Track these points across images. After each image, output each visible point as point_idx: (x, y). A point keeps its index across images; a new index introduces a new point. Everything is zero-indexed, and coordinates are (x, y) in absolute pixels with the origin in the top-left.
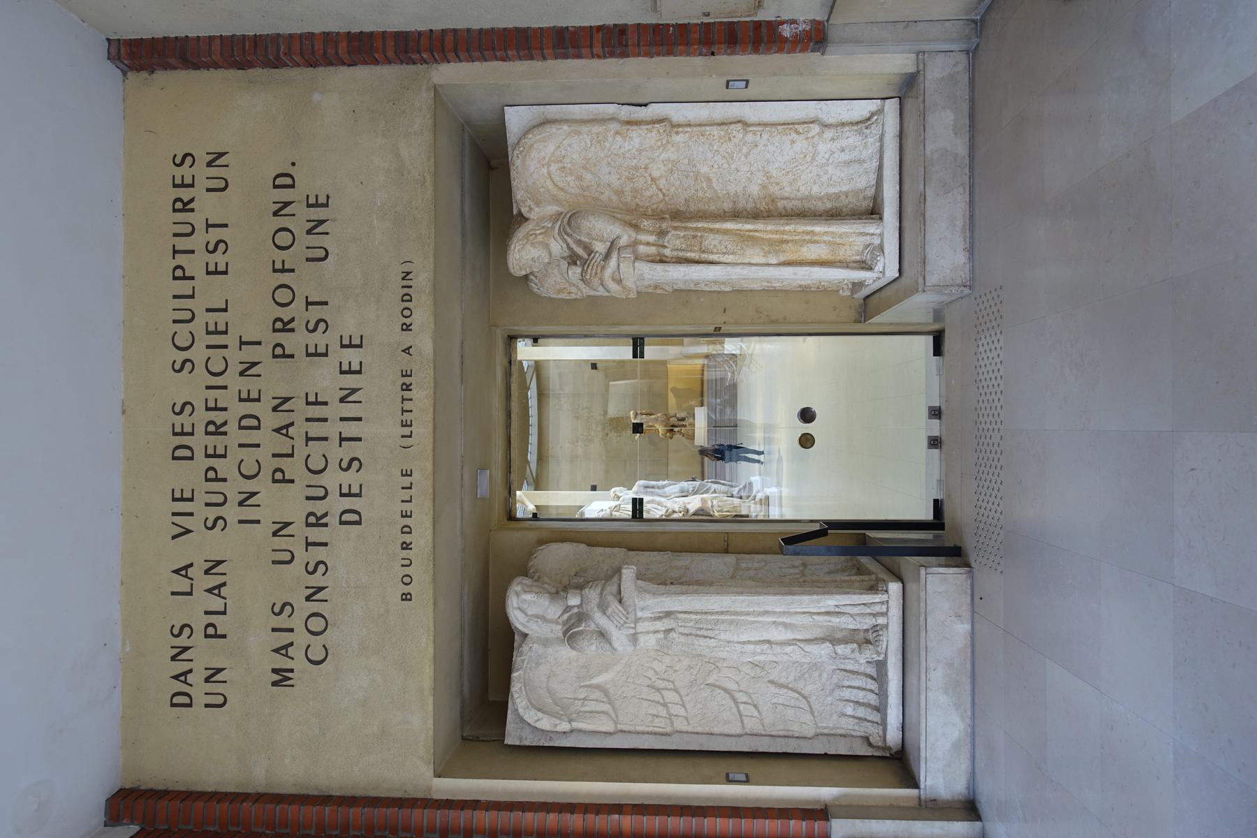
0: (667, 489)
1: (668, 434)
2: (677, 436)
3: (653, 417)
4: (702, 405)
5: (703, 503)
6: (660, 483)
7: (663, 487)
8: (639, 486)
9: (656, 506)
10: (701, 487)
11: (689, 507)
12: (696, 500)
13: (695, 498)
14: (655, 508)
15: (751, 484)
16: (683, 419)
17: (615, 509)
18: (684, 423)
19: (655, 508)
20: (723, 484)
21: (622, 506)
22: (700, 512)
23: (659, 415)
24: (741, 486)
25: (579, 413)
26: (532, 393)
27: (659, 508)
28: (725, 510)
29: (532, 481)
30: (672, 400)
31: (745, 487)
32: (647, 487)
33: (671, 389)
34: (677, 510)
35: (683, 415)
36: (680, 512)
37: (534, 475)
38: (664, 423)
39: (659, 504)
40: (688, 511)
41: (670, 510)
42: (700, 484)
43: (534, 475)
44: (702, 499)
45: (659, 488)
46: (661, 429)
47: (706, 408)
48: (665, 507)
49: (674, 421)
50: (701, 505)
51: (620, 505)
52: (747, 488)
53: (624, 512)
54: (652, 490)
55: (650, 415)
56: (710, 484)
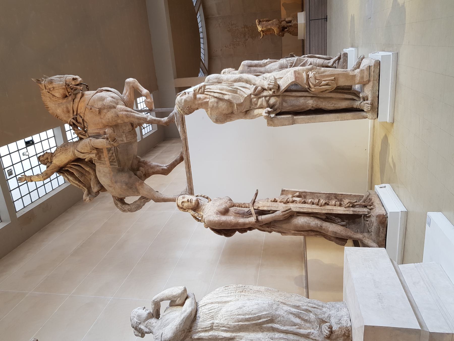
0: (267, 67)
1: (281, 33)
2: (287, 35)
3: (271, 22)
4: (302, 11)
5: (296, 78)
6: (265, 61)
7: (265, 65)
8: (244, 65)
9: (244, 84)
10: (298, 62)
11: (280, 82)
12: (289, 73)
13: (287, 72)
14: (244, 87)
15: (346, 55)
16: (290, 22)
17: (200, 91)
18: (290, 24)
19: (244, 87)
20: (319, 58)
21: (207, 87)
22: (293, 88)
23: (274, 20)
24: (337, 57)
25: (230, 28)
26: (200, 19)
27: (248, 86)
28: (323, 83)
29: (206, 72)
30: (283, 12)
31: (339, 59)
32: (250, 66)
33: (283, 4)
34: (266, 87)
35: (289, 19)
36: (271, 90)
37: (207, 68)
38: (278, 26)
39: (247, 82)
40: (279, 87)
41: (259, 88)
42: (297, 60)
43: (207, 68)
44: (295, 71)
45: (261, 66)
46: (276, 30)
47: (305, 12)
48: (254, 85)
49: (284, 23)
50: (294, 80)
51: (205, 86)
52: (342, 60)
53: (209, 93)
54: (255, 68)
55: (269, 21)
56: (306, 59)
